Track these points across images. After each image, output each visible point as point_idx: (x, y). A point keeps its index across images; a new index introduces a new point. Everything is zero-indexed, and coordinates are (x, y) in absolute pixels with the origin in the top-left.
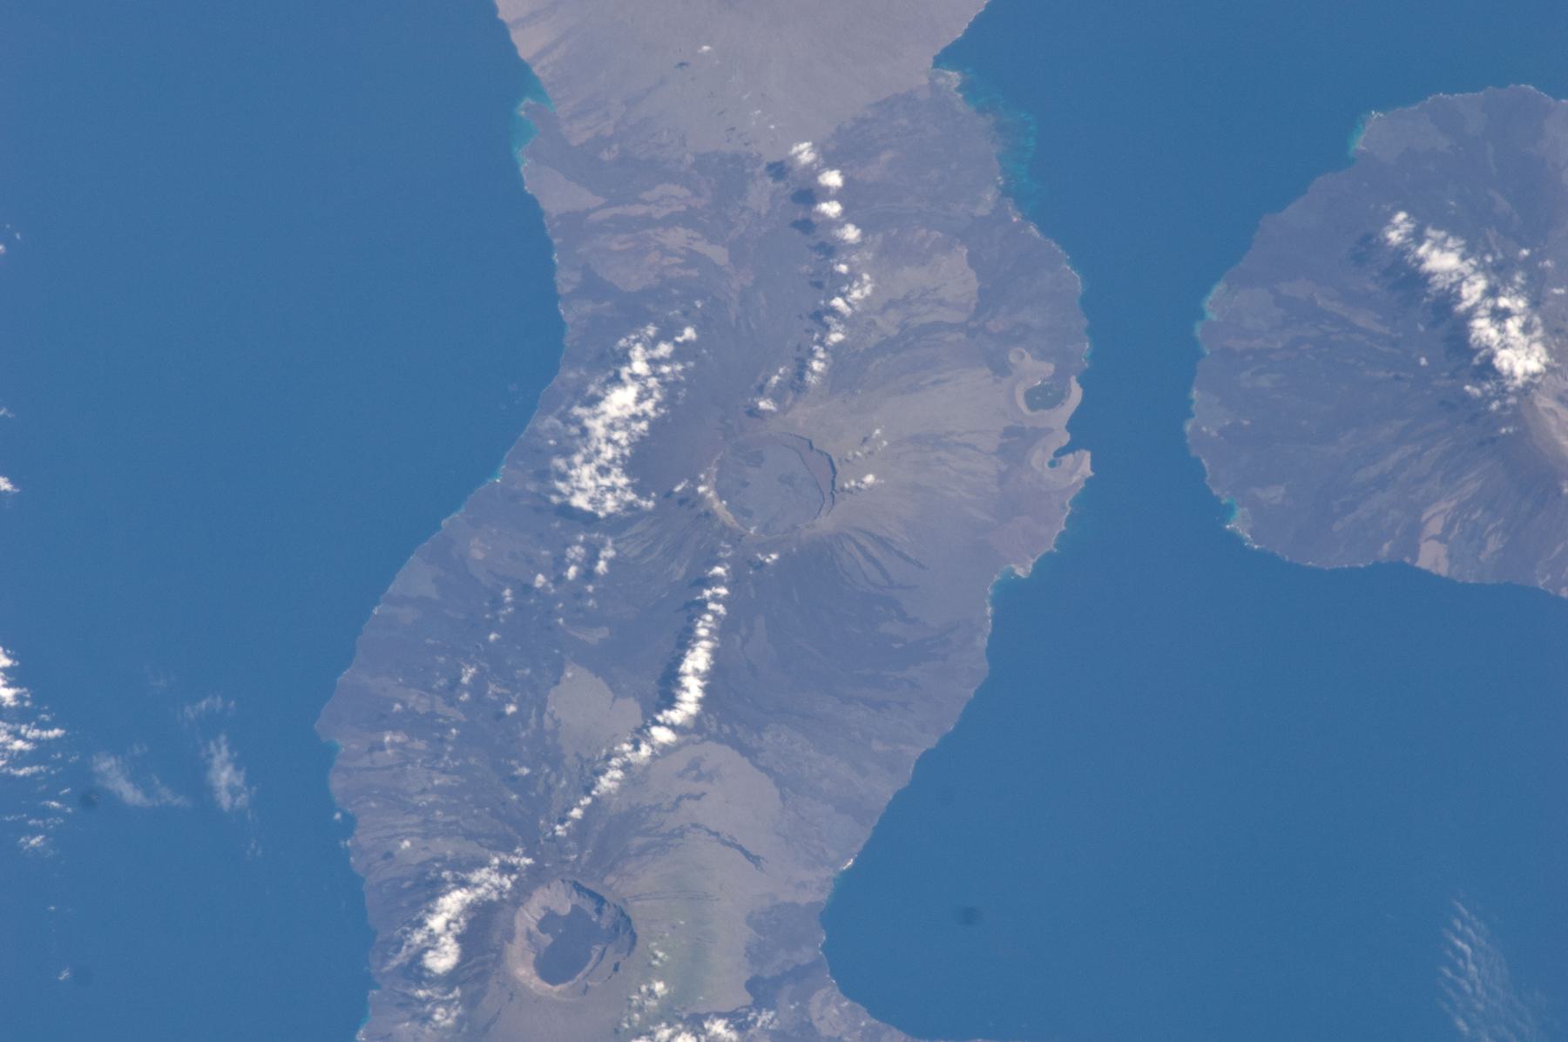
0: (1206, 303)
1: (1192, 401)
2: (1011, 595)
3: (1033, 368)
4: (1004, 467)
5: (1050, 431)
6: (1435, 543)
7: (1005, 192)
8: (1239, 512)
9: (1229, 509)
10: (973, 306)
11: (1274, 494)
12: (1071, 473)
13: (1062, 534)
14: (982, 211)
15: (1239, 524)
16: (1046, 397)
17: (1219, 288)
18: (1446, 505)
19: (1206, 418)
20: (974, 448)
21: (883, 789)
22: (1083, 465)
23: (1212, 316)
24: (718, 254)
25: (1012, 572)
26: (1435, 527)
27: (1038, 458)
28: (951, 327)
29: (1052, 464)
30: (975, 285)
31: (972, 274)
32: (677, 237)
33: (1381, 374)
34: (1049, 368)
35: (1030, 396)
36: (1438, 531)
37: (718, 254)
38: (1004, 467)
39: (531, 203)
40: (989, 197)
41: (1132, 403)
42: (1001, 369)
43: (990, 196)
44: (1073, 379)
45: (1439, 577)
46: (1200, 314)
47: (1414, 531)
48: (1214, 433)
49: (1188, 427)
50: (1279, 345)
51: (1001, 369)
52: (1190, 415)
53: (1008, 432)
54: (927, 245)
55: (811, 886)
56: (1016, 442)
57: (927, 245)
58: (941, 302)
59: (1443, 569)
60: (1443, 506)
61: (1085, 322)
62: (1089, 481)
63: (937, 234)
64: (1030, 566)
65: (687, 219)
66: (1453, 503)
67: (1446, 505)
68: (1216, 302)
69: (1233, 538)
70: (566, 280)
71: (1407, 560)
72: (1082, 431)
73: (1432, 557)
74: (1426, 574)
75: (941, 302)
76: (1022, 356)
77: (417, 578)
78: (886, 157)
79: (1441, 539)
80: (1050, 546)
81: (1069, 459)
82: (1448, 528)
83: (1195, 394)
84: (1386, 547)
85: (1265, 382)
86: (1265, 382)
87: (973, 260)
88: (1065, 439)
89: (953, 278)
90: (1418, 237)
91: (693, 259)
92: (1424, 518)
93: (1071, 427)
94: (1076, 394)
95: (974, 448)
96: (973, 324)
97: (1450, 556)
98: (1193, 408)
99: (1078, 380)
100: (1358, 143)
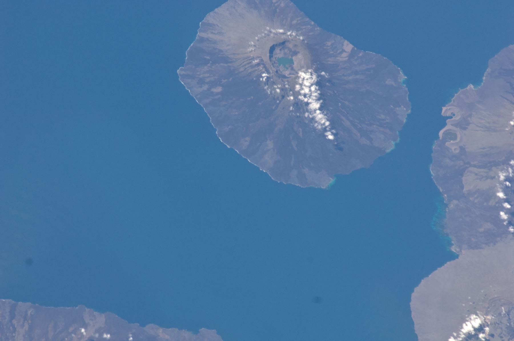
0: (393, 147)
1: (407, 119)
2: (477, 81)
3: (452, 146)
4: (469, 119)
5: (452, 125)
6: (346, 50)
7: (446, 205)
8: (402, 81)
9: (405, 82)
10: (466, 172)
11: (389, 82)
12: (449, 109)
13: (456, 93)
14: (455, 202)
15: (403, 77)
17: (388, 151)
18: (339, 59)
19: (403, 112)
20: (477, 126)
22: (445, 111)
23: (393, 143)
25: (474, 87)
26: (344, 55)
27: (457, 118)
28: (475, 166)
29: (454, 115)
30: (464, 179)
31: (463, 183)
33: (347, 103)
34: (447, 144)
35: (455, 138)
36: (344, 53)
38: (469, 119)
40: (452, 206)
41: (425, 125)
42: (462, 149)
43: (452, 206)
44: (441, 138)
45: (348, 40)
46: (396, 144)
47: (352, 55)
48: (402, 106)
49: (410, 111)
50: (375, 126)
51: (462, 149)
52: (408, 115)
53: (465, 129)
54: (476, 196)
56: (463, 125)
57: (476, 196)
58: (476, 174)
59: (346, 42)
60: (341, 59)
61: (432, 155)
62: (444, 106)
63: (471, 199)
64: (468, 87)
66: (337, 58)
67: (339, 59)
68: (390, 147)
69: (405, 73)
71: (356, 49)
72: (442, 122)
73: (348, 47)
74: (351, 43)
75: (476, 174)
76: (455, 149)
78: (482, 230)
79: (343, 51)
80: (461, 90)
81: (448, 114)
82: (341, 53)
83: (405, 121)
84: (361, 55)
85: (383, 116)
86: (383, 116)
87: (462, 187)
88: (448, 121)
89: (471, 182)
90: (325, 130)
92: (347, 58)
93: (445, 125)
94: (441, 133)
95: (477, 126)
96: (468, 166)
97: (343, 45)
98: (406, 116)
99: (439, 138)
100: (332, 181)
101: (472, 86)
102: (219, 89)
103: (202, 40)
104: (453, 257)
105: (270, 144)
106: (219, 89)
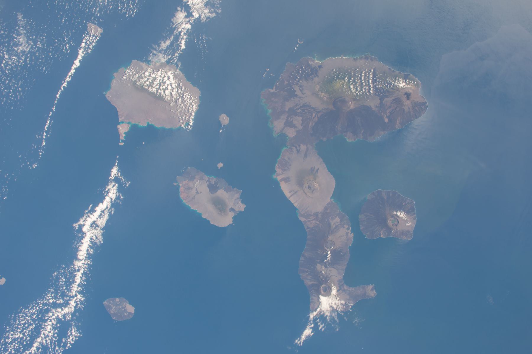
11: (368, 233)
16: (348, 229)
19: (362, 227)
21: (345, 267)
24: (318, 222)
27: (349, 234)
32: (314, 221)
37: (318, 222)
39: (300, 221)
42: (344, 227)
51: (344, 227)
55: (341, 277)
56: (347, 234)
65: (314, 220)
70: (306, 228)
72: (352, 231)
73: (382, 236)
77: (302, 258)
91: (316, 223)
101: (350, 245)
102: (404, 204)
103: (414, 214)
104: (331, 198)
105: (385, 198)
106: (404, 204)
